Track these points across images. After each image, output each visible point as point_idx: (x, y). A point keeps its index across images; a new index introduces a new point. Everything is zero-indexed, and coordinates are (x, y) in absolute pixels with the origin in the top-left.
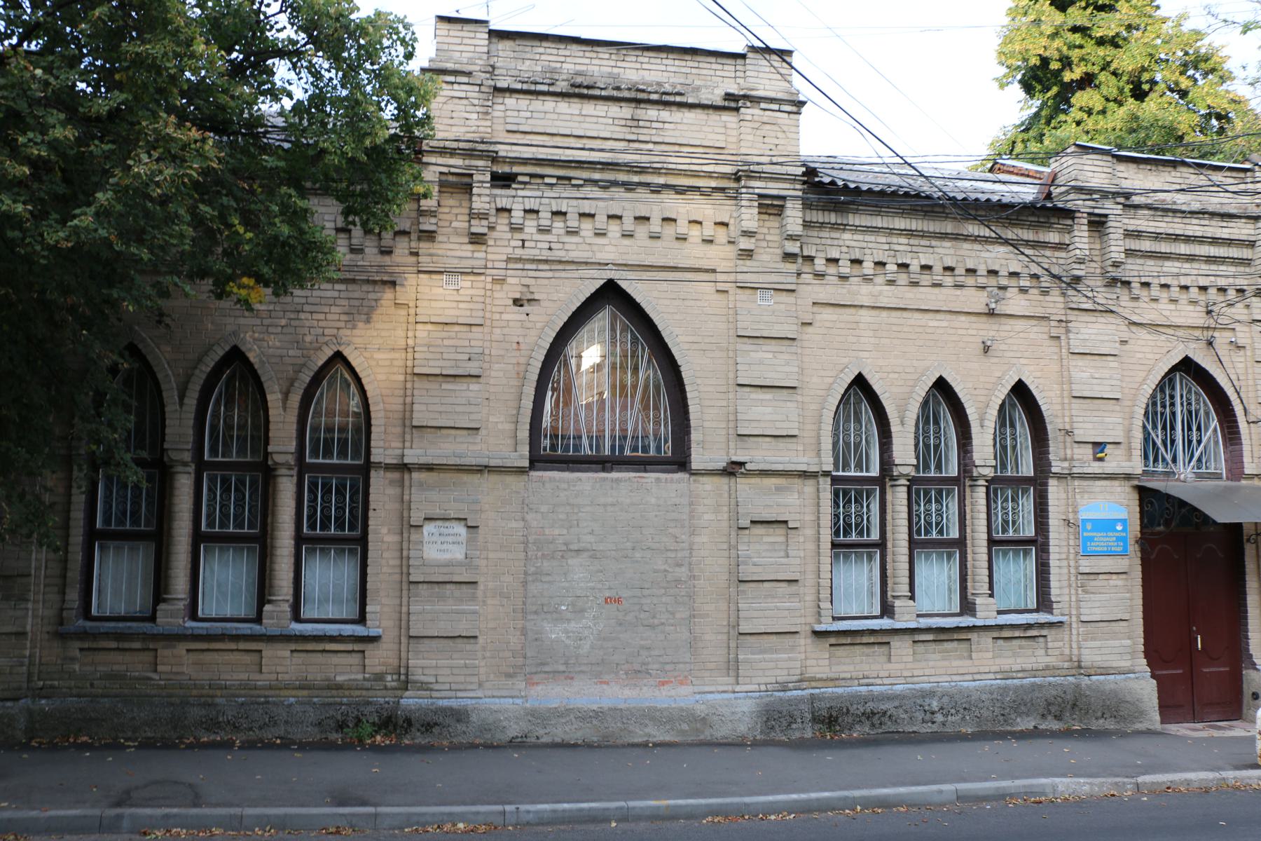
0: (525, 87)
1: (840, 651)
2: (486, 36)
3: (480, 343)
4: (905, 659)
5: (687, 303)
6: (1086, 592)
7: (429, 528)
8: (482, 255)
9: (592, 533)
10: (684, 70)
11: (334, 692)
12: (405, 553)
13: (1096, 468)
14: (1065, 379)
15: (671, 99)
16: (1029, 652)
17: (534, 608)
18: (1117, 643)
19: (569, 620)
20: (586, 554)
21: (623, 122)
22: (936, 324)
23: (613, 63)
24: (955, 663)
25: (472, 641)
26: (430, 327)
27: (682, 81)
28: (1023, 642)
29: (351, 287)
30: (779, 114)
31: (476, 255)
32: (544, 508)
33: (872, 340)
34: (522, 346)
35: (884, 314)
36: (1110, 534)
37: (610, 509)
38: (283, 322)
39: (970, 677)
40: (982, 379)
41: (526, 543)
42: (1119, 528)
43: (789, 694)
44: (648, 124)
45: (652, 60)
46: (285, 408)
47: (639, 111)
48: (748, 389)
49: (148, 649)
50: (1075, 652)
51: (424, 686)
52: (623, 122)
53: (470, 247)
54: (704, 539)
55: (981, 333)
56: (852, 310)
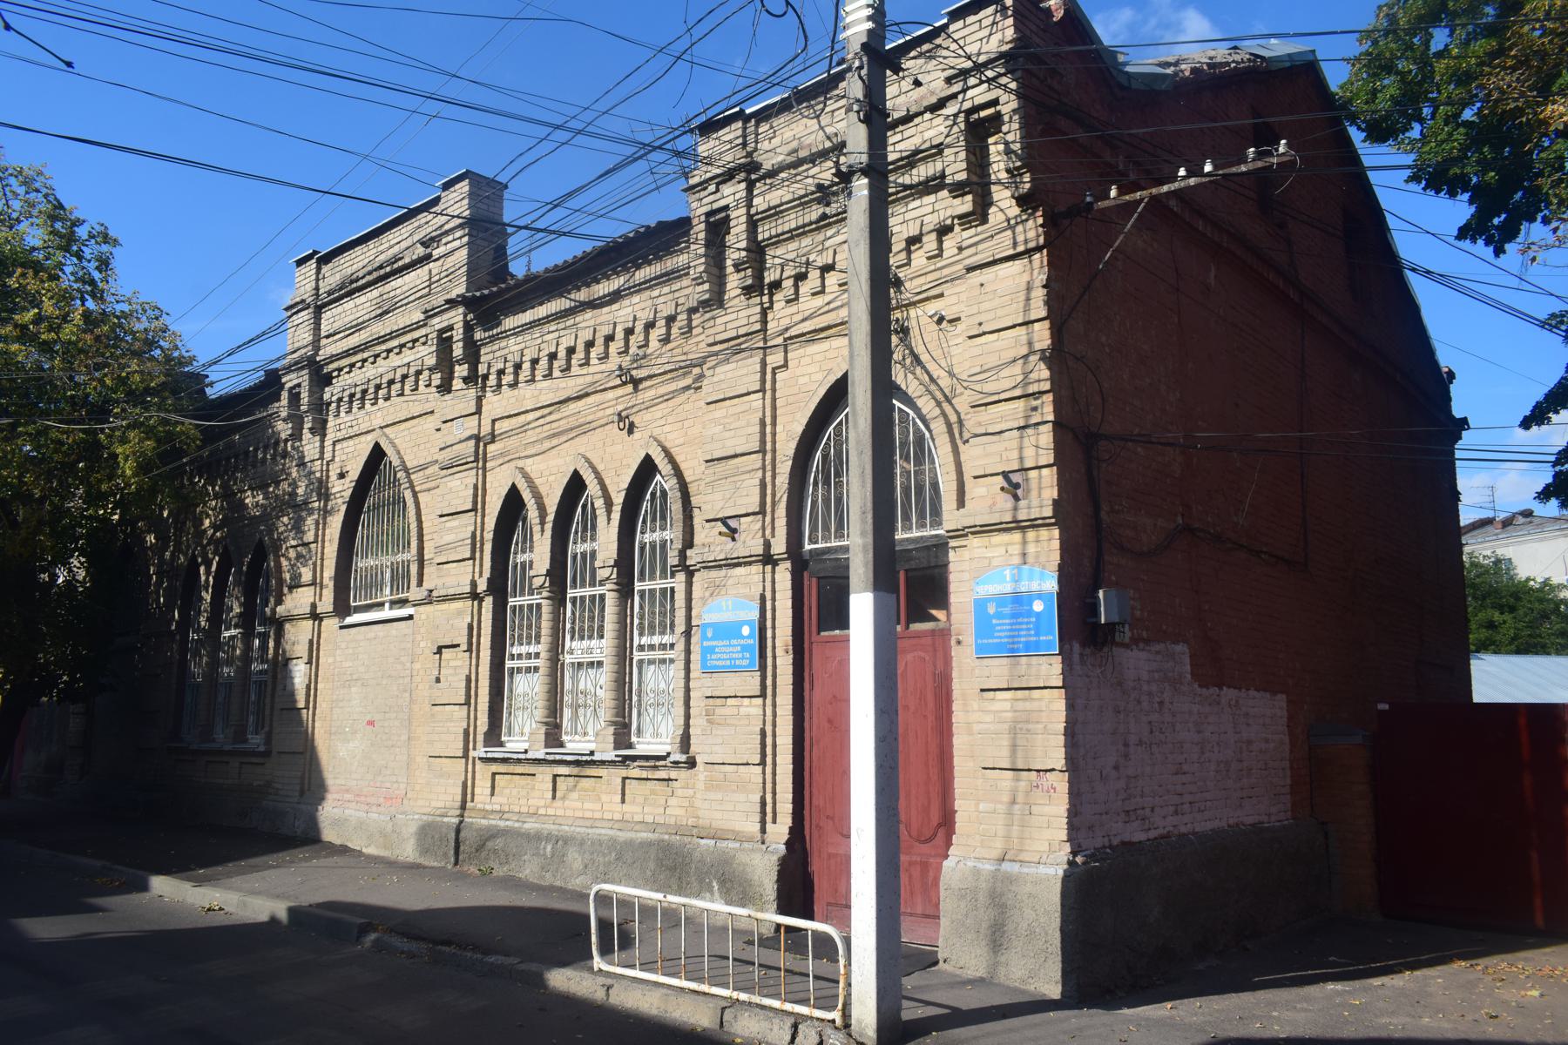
18: (742, 797)
24: (587, 805)
36: (734, 642)
39: (588, 823)
42: (746, 631)
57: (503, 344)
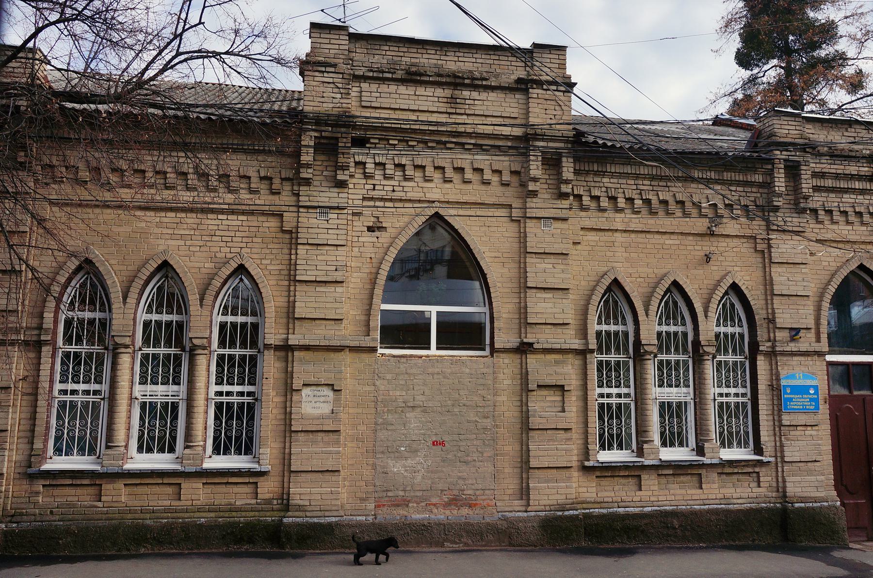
0: (375, 75)
1: (605, 482)
2: (347, 38)
3: (344, 258)
4: (652, 488)
5: (492, 229)
6: (788, 440)
7: (306, 391)
8: (345, 195)
9: (423, 394)
10: (488, 62)
11: (234, 514)
12: (288, 409)
13: (792, 347)
14: (768, 283)
15: (480, 83)
16: (746, 484)
17: (381, 449)
18: (813, 478)
19: (406, 459)
20: (419, 409)
21: (445, 100)
22: (671, 242)
23: (437, 57)
24: (689, 492)
25: (336, 474)
26: (307, 247)
27: (487, 70)
28: (741, 477)
29: (250, 218)
30: (556, 93)
31: (340, 195)
32: (389, 377)
33: (625, 255)
34: (374, 260)
35: (633, 235)
37: (435, 376)
38: (201, 243)
40: (705, 282)
41: (376, 402)
43: (566, 513)
44: (463, 101)
45: (466, 55)
46: (201, 305)
47: (456, 92)
48: (535, 291)
49: (95, 485)
50: (781, 485)
51: (300, 508)
52: (445, 100)
53: (336, 190)
54: (504, 398)
55: (705, 248)
56: (610, 233)
57: (596, 179)
